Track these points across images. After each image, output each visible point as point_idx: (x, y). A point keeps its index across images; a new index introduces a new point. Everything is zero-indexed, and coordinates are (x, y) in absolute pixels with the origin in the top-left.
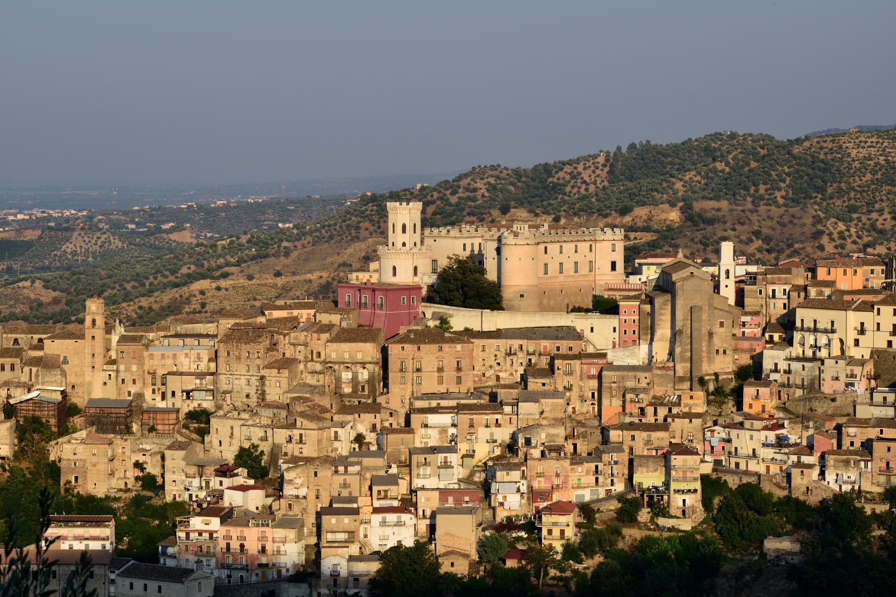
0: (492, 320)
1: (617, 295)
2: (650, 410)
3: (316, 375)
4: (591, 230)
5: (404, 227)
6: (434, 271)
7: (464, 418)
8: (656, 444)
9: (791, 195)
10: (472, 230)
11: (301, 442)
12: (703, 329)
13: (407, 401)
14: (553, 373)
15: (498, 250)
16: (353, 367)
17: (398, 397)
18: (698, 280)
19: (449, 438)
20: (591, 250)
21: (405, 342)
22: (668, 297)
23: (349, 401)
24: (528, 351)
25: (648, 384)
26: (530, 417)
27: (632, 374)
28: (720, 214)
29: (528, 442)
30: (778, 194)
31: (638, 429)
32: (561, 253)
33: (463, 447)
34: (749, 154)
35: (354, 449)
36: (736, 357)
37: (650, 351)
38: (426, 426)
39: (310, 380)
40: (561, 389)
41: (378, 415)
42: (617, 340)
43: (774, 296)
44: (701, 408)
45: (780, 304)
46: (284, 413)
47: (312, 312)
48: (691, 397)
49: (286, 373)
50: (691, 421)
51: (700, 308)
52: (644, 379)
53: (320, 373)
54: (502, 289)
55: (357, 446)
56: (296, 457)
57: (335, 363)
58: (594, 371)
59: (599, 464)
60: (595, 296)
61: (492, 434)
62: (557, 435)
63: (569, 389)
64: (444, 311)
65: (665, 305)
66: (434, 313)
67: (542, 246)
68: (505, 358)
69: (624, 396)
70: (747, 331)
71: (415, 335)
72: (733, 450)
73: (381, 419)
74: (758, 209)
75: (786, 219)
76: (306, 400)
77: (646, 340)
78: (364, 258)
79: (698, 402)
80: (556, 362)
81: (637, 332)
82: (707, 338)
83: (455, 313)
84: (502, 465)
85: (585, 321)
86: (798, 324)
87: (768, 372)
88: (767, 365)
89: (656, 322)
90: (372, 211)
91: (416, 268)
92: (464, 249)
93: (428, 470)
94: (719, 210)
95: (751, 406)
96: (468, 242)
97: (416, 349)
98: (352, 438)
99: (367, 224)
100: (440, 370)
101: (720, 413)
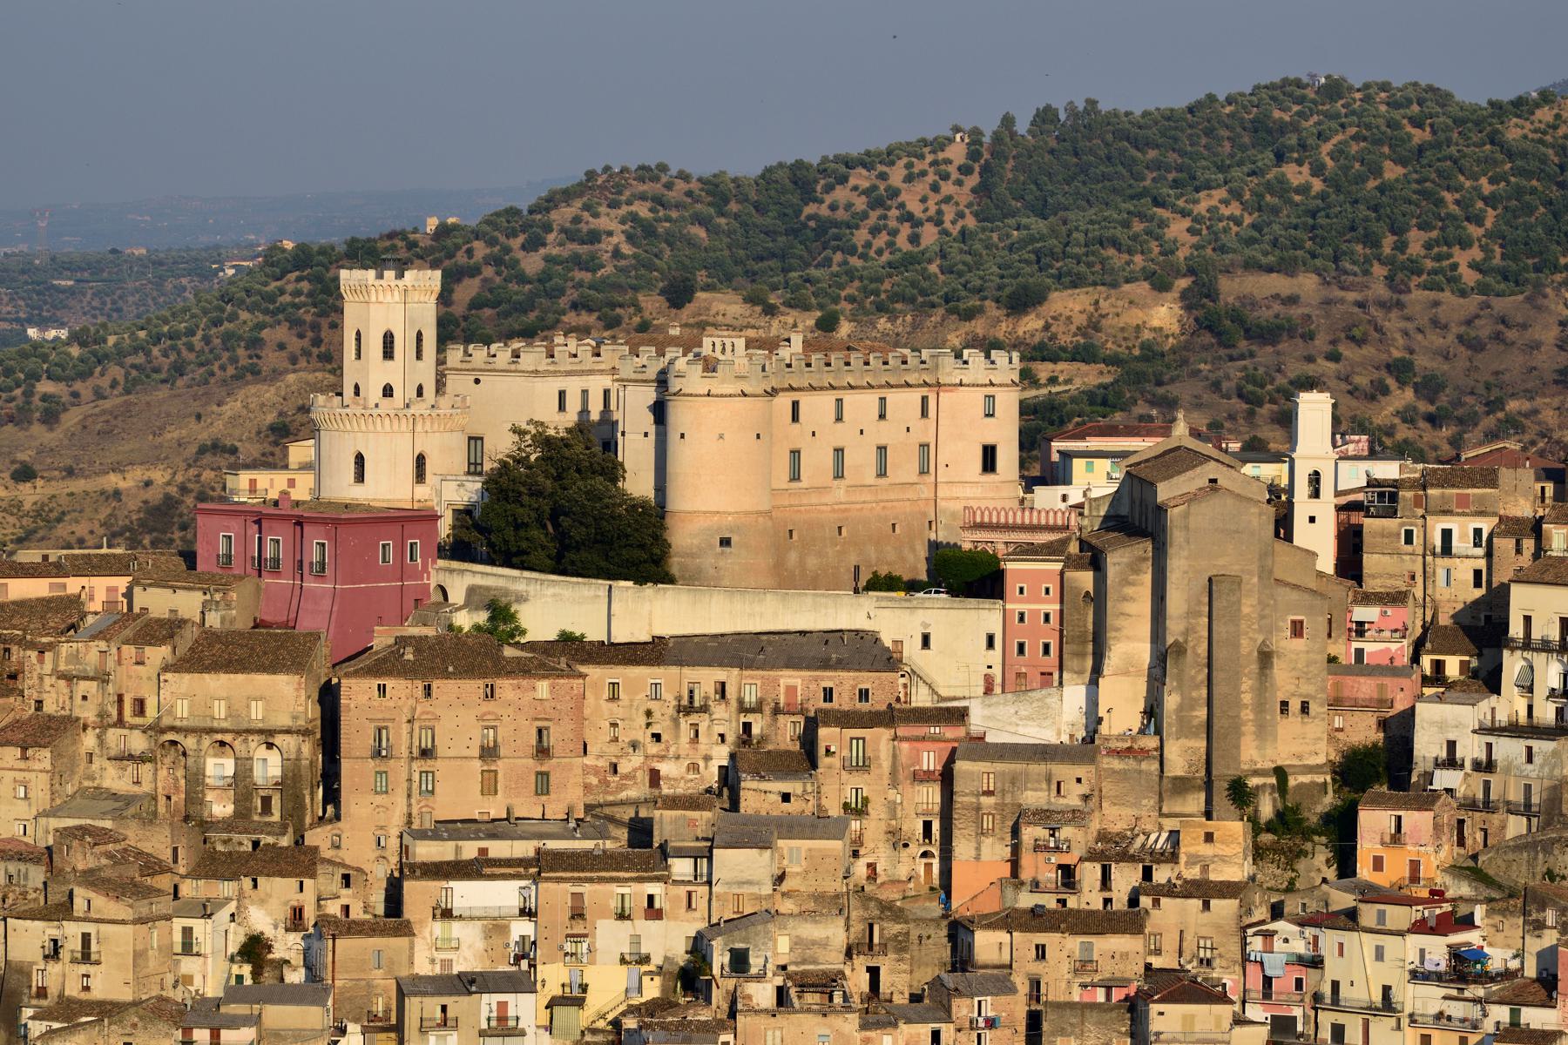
0: (641, 612)
1: (999, 542)
2: (1090, 874)
3: (131, 767)
4: (925, 354)
5: (388, 340)
6: (474, 468)
7: (556, 894)
8: (1107, 970)
9: (1497, 261)
10: (585, 352)
11: (86, 957)
12: (1244, 642)
13: (394, 843)
14: (814, 766)
15: (659, 411)
16: (237, 744)
17: (366, 829)
18: (1230, 501)
19: (513, 950)
20: (924, 413)
21: (389, 673)
22: (1145, 547)
23: (225, 842)
24: (741, 702)
25: (1086, 798)
26: (746, 890)
27: (1037, 769)
28: (1296, 312)
29: (739, 962)
30: (1462, 258)
31: (1054, 928)
32: (839, 419)
33: (553, 976)
34: (1378, 142)
35: (240, 978)
36: (1338, 722)
37: (1093, 702)
38: (447, 914)
39: (115, 779)
40: (835, 811)
41: (308, 882)
42: (997, 672)
43: (1447, 550)
44: (1236, 870)
45: (1463, 571)
46: (37, 875)
47: (122, 583)
49: (43, 758)
50: (1206, 906)
51: (1237, 581)
52: (1074, 782)
53: (142, 759)
54: (669, 521)
55: (246, 970)
56: (71, 1001)
58: (930, 761)
60: (934, 546)
61: (636, 940)
62: (824, 944)
63: (858, 809)
64: (501, 583)
65: (1137, 571)
66: (471, 591)
67: (784, 402)
68: (676, 722)
69: (1015, 832)
70: (1369, 648)
71: (418, 651)
72: (1327, 990)
73: (318, 894)
74: (1403, 297)
75: (1484, 329)
76: (101, 836)
77: (1080, 672)
78: (273, 428)
79: (1227, 851)
80: (823, 732)
81: (1054, 650)
82: (1254, 667)
83: (532, 589)
84: (664, 1027)
85: (904, 616)
86: (1516, 629)
87: (1430, 766)
88: (1427, 746)
89: (1111, 621)
90: (297, 293)
91: (420, 461)
92: (562, 407)
94: (1292, 300)
95: (1378, 864)
96: (573, 386)
97: (420, 692)
98: (233, 948)
99: (281, 333)
100: (489, 753)
101: (1292, 882)
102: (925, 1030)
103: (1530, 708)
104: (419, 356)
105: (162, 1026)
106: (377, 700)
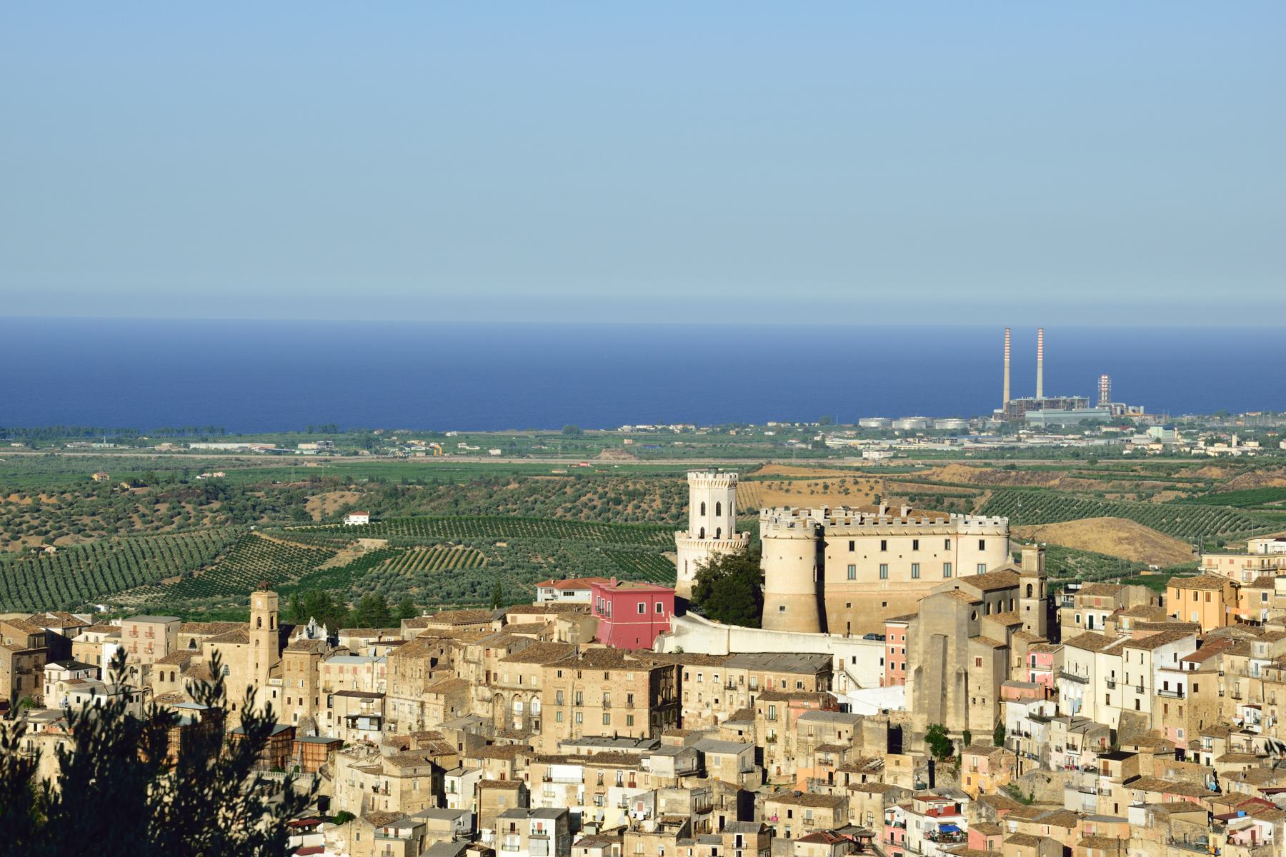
7: (594, 772)
25: (850, 740)
38: (550, 780)
48: (898, 763)
57: (503, 689)
59: (717, 846)
70: (1038, 674)
85: (844, 647)
93: (517, 840)
100: (606, 705)
102: (708, 848)
103: (1057, 708)
104: (718, 513)
105: (371, 827)
106: (557, 679)
